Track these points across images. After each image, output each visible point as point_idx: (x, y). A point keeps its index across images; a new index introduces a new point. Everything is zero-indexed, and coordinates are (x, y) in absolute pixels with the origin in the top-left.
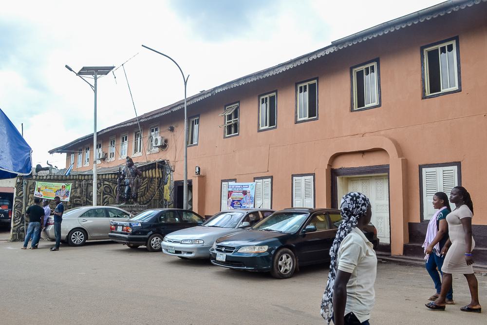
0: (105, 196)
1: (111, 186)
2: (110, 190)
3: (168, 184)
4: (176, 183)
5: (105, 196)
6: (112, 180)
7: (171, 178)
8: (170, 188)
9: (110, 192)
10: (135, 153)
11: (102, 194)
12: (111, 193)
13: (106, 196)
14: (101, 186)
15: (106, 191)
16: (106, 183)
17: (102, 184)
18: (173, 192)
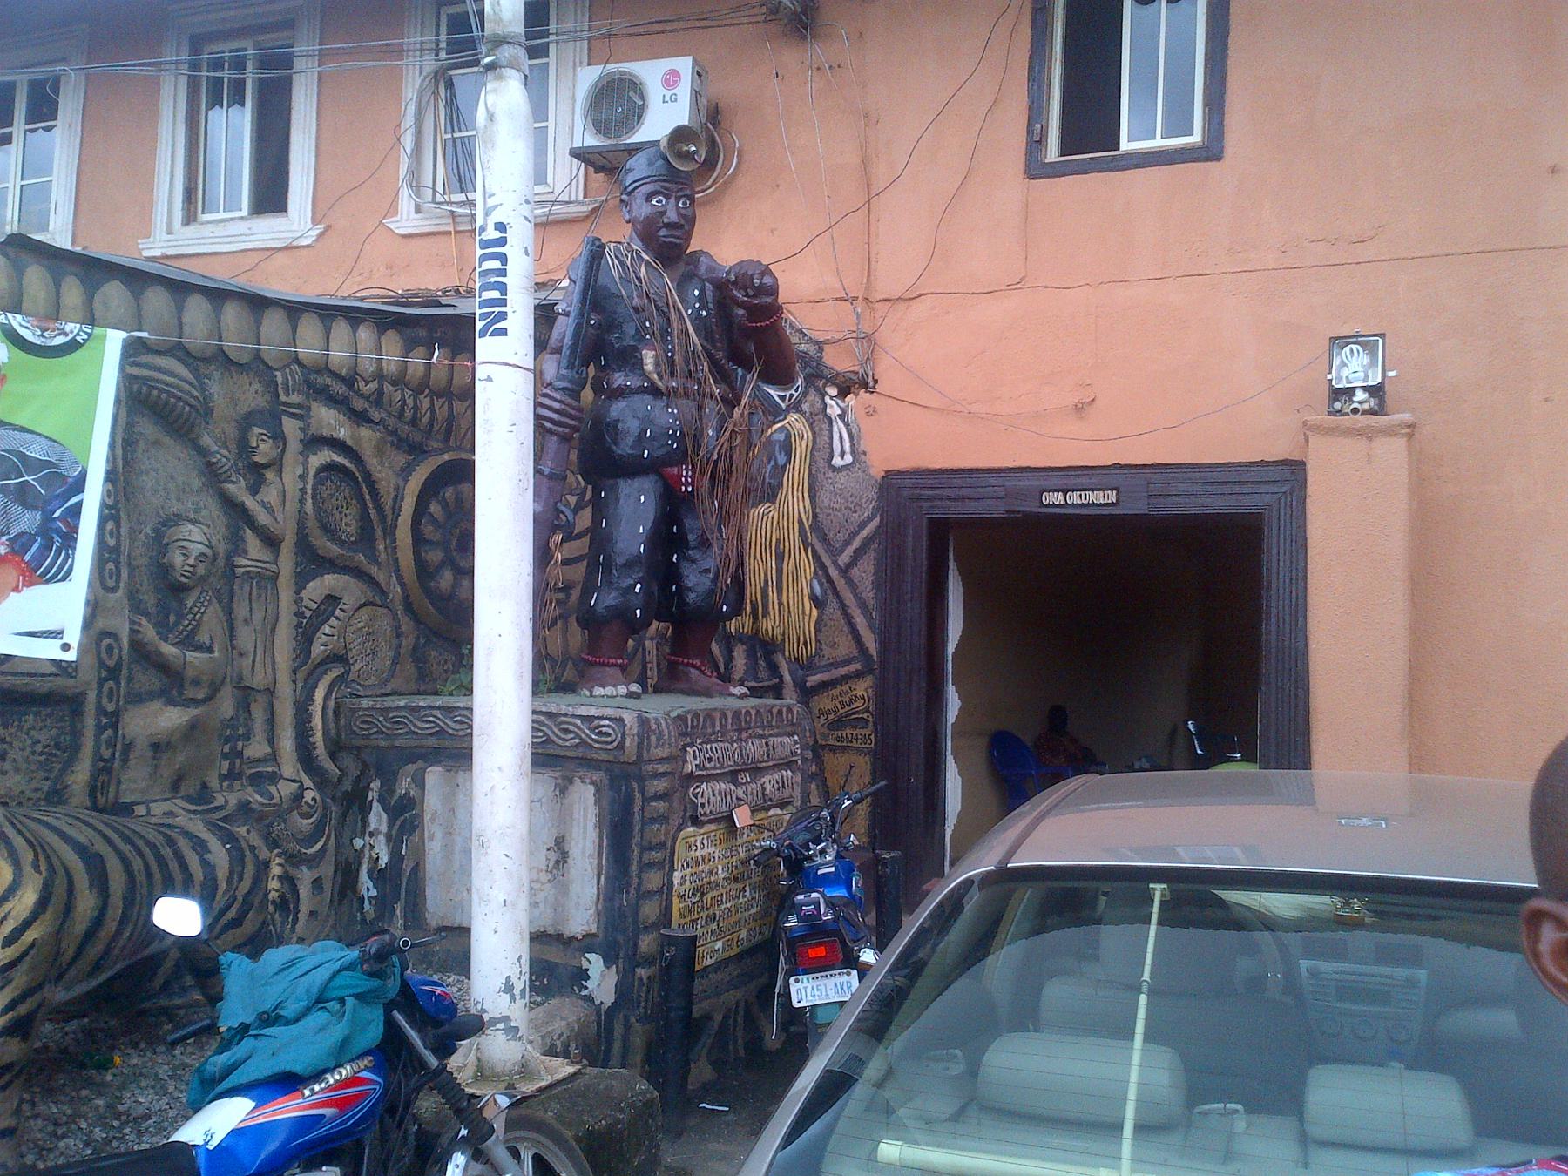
0: (316, 589)
1: (372, 462)
2: (364, 516)
3: (795, 501)
4: (900, 490)
5: (316, 589)
6: (378, 399)
7: (821, 452)
8: (816, 533)
9: (366, 537)
10: (190, 218)
11: (286, 563)
12: (373, 558)
13: (329, 582)
14: (277, 464)
15: (330, 532)
16: (328, 420)
17: (290, 426)
18: (865, 573)
